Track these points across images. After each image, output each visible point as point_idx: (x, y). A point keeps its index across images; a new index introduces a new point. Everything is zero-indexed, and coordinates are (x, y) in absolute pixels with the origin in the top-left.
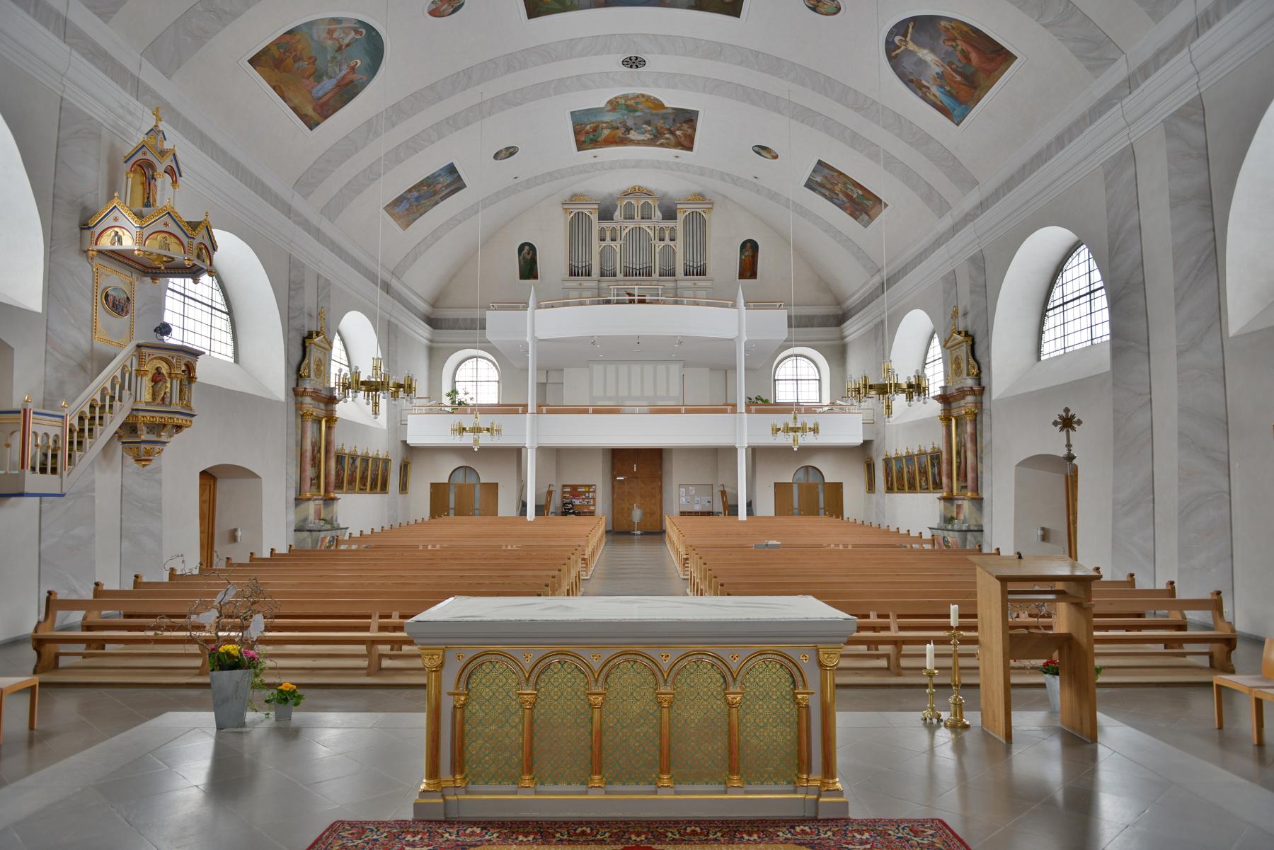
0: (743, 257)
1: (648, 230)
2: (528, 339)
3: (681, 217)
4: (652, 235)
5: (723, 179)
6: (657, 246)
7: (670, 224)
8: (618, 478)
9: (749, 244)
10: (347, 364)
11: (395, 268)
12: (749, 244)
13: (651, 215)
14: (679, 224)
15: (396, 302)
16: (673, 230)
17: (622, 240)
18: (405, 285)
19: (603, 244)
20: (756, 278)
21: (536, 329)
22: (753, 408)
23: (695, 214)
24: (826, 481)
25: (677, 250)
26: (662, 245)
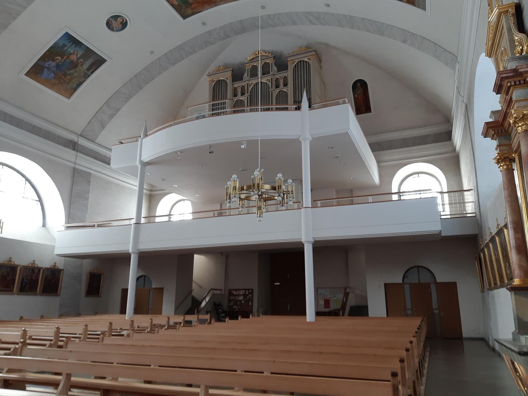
0: (356, 96)
1: (268, 82)
2: (138, 163)
3: (291, 67)
4: (270, 85)
5: (311, 23)
6: (274, 92)
7: (283, 74)
8: (275, 284)
9: (359, 84)
10: (38, 199)
11: (82, 132)
12: (359, 84)
13: (269, 71)
14: (289, 74)
15: (79, 154)
16: (285, 78)
17: (249, 92)
18: (100, 145)
19: (236, 99)
20: (371, 112)
21: (142, 154)
22: (319, 203)
23: (302, 62)
24: (438, 281)
25: (289, 93)
26: (278, 91)
